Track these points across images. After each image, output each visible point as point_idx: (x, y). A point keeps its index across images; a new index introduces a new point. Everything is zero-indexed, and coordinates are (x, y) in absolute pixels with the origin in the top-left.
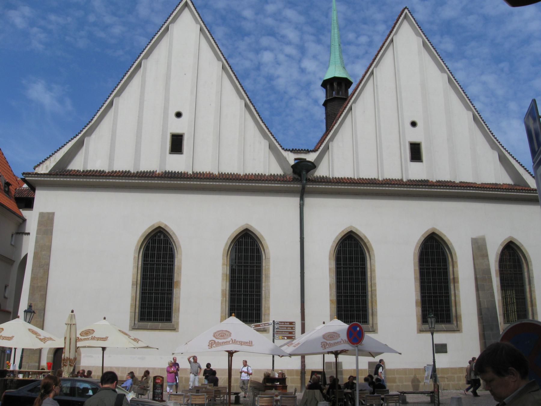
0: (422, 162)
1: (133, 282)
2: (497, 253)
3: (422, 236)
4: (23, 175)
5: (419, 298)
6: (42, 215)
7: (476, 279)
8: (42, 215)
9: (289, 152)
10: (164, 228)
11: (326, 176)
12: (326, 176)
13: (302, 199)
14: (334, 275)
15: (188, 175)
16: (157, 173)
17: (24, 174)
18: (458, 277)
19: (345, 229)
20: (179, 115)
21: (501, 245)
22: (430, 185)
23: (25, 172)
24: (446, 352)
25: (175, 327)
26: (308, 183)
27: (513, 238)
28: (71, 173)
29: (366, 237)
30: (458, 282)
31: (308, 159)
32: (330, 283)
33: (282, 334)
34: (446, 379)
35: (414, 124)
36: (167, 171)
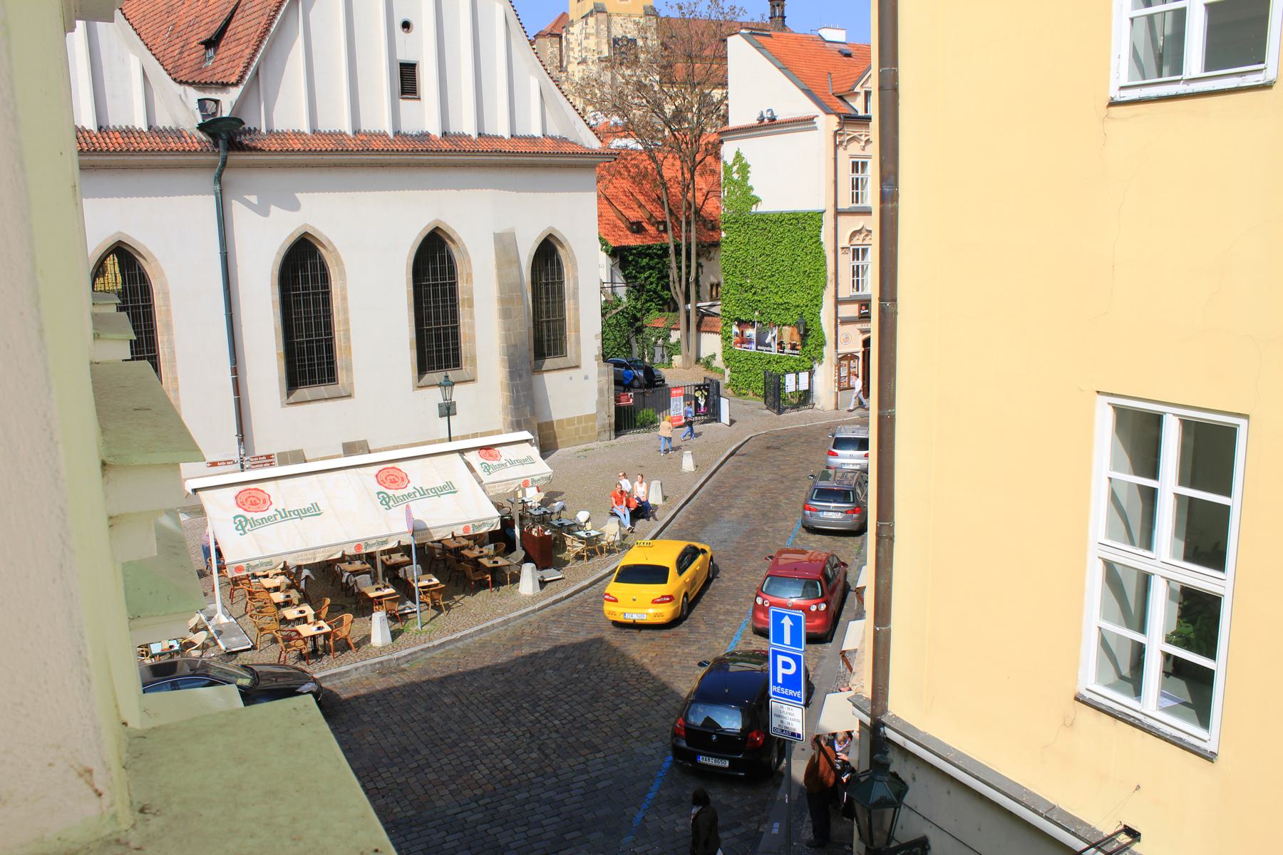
2: (529, 255)
13: (219, 179)
21: (536, 241)
27: (554, 229)
29: (330, 242)
32: (275, 325)
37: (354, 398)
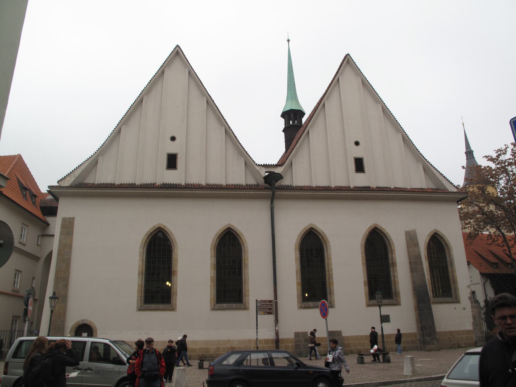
0: (364, 172)
1: (139, 272)
3: (367, 230)
4: (48, 188)
5: (366, 279)
6: (64, 220)
7: (410, 263)
8: (64, 220)
9: (261, 167)
10: (164, 229)
11: (290, 185)
12: (290, 185)
13: (272, 203)
14: (299, 263)
15: (181, 186)
16: (157, 184)
17: (49, 187)
18: (396, 262)
19: (306, 226)
20: (173, 139)
21: (428, 236)
22: (372, 190)
23: (51, 185)
24: (389, 321)
26: (277, 191)
27: (437, 230)
28: (88, 185)
30: (396, 266)
31: (276, 172)
33: (264, 310)
34: (390, 343)
35: (357, 143)
36: (165, 183)
37: (335, 308)
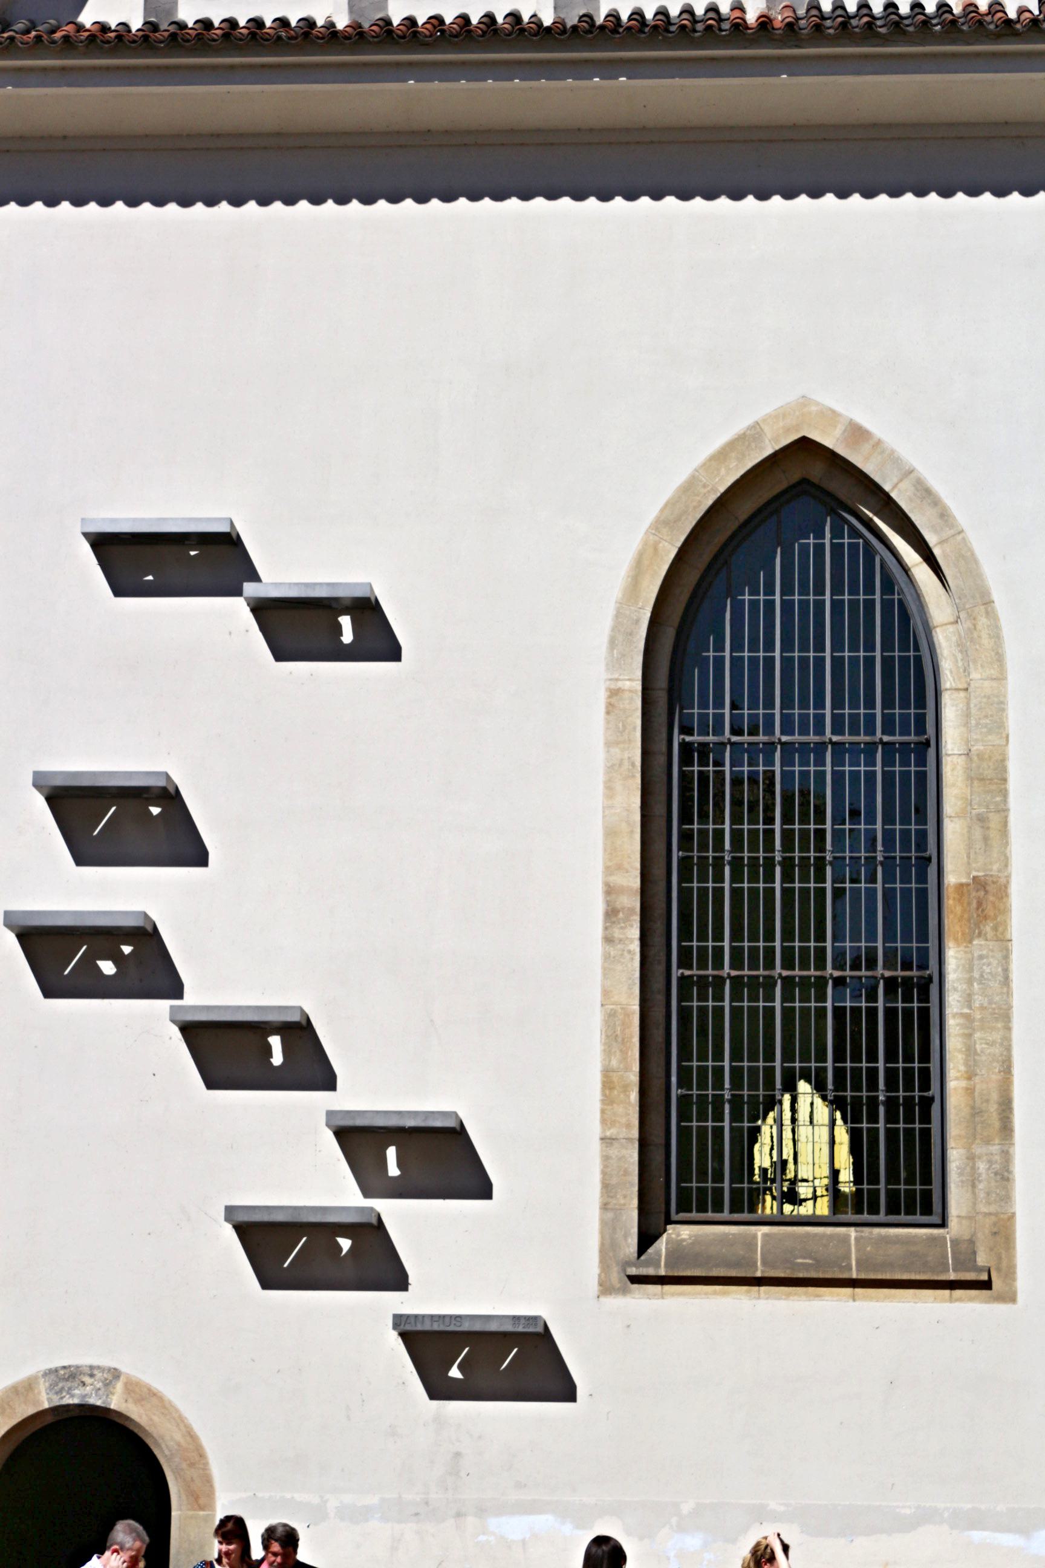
25: (982, 1260)
